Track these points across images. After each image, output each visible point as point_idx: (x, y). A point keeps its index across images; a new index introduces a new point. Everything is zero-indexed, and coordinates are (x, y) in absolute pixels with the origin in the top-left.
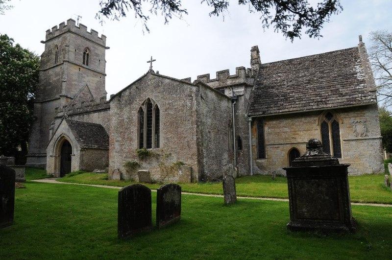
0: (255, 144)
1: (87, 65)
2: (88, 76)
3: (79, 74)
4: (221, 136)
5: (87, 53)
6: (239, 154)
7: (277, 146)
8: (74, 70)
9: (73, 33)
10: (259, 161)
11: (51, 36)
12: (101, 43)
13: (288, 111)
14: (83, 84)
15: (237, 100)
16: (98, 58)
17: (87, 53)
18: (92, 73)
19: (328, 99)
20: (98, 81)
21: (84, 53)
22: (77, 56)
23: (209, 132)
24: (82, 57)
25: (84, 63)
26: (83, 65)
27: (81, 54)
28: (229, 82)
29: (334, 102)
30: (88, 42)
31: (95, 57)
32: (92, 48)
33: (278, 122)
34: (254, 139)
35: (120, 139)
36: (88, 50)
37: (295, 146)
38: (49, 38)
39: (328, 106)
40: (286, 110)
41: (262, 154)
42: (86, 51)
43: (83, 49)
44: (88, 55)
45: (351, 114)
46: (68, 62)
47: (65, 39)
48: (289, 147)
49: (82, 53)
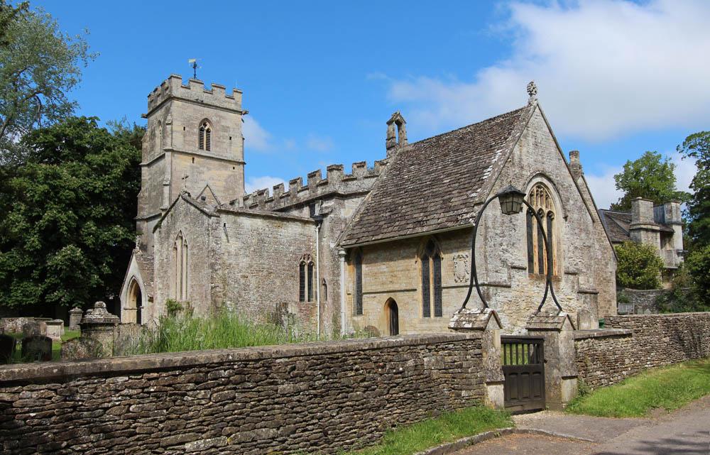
0: (351, 291)
1: (208, 149)
2: (209, 169)
3: (193, 168)
4: (278, 282)
5: (206, 128)
6: (324, 307)
7: (373, 295)
8: (183, 164)
9: (178, 99)
10: (355, 318)
11: (153, 105)
12: (233, 107)
13: (381, 239)
14: (203, 185)
15: (321, 222)
16: (226, 134)
17: (206, 128)
18: (217, 163)
19: (429, 218)
20: (230, 176)
21: (202, 130)
22: (188, 138)
23: (244, 277)
24: (196, 138)
25: (201, 147)
26: (200, 152)
27: (194, 134)
28: (320, 191)
29: (436, 222)
30: (206, 109)
31: (222, 133)
32: (214, 119)
33: (376, 255)
34: (351, 284)
35: (161, 286)
36: (207, 123)
37: (391, 295)
38: (151, 109)
39: (425, 229)
40: (380, 237)
41: (359, 311)
42: (205, 125)
43: (197, 123)
44: (208, 131)
45: (454, 243)
46: (172, 151)
47: (168, 111)
48: (386, 297)
49: (196, 130)
